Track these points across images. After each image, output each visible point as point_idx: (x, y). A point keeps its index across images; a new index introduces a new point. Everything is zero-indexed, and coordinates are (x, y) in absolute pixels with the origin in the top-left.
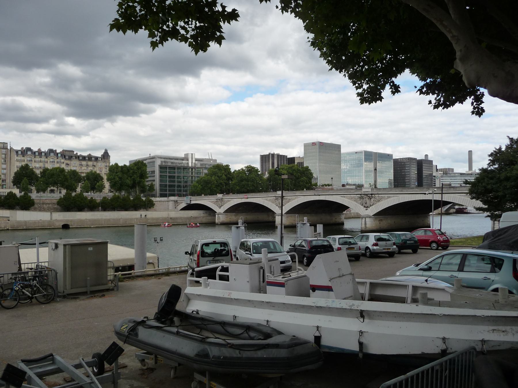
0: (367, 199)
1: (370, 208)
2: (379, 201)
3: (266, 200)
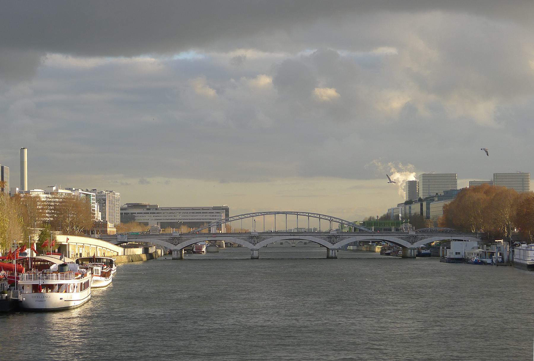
0: (334, 238)
2: (342, 240)
3: (238, 238)
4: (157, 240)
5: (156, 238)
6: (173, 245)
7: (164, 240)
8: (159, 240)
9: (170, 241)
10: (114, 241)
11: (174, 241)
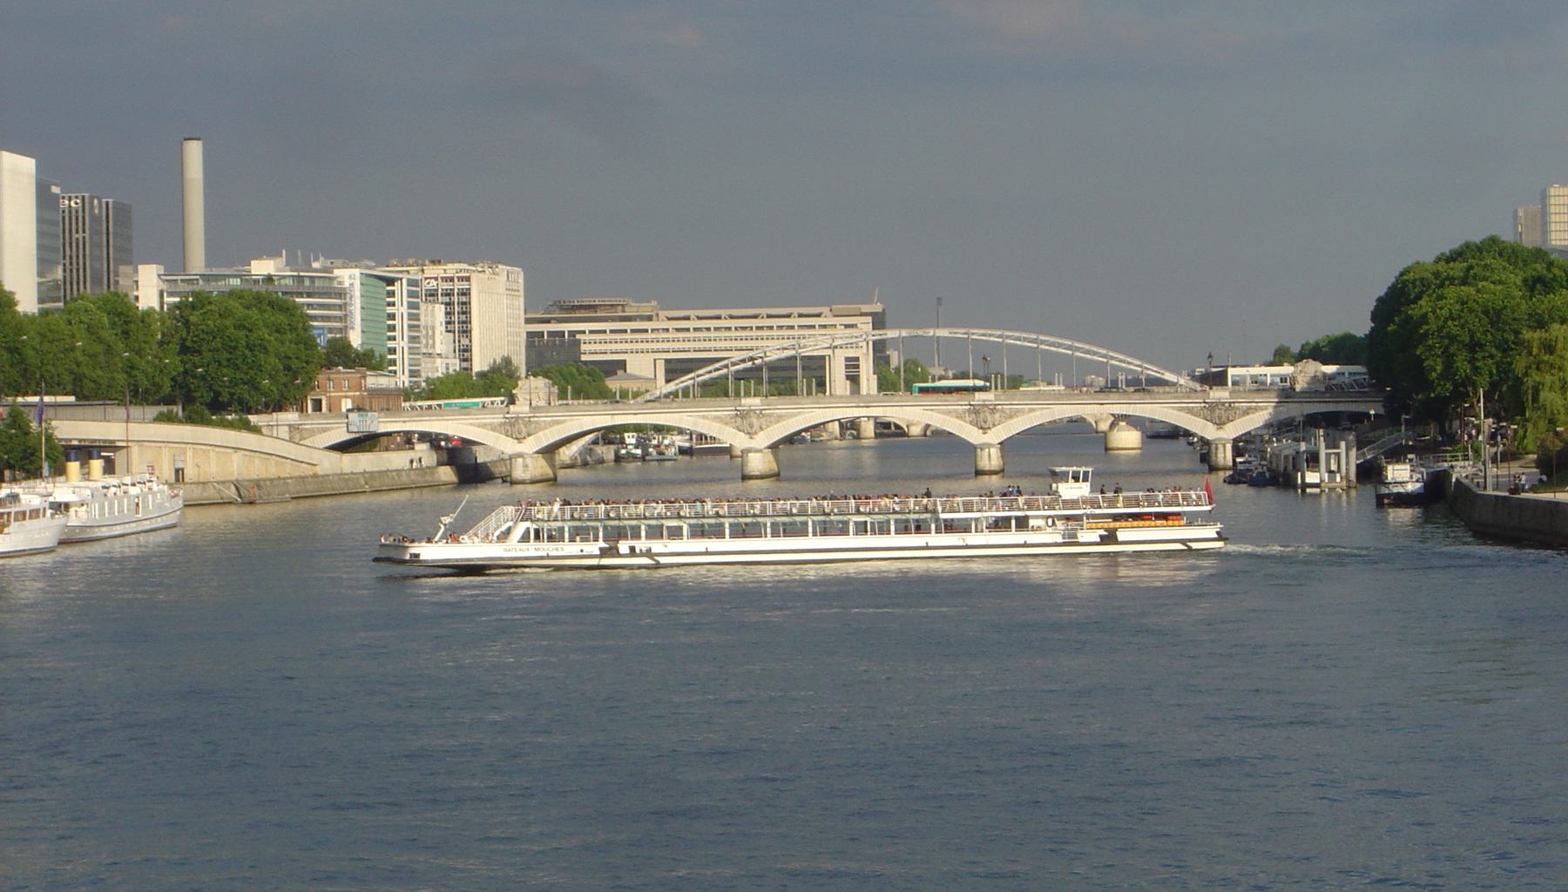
0: (988, 415)
1: (993, 429)
2: (1011, 417)
3: (704, 417)
5: (463, 421)
7: (485, 425)
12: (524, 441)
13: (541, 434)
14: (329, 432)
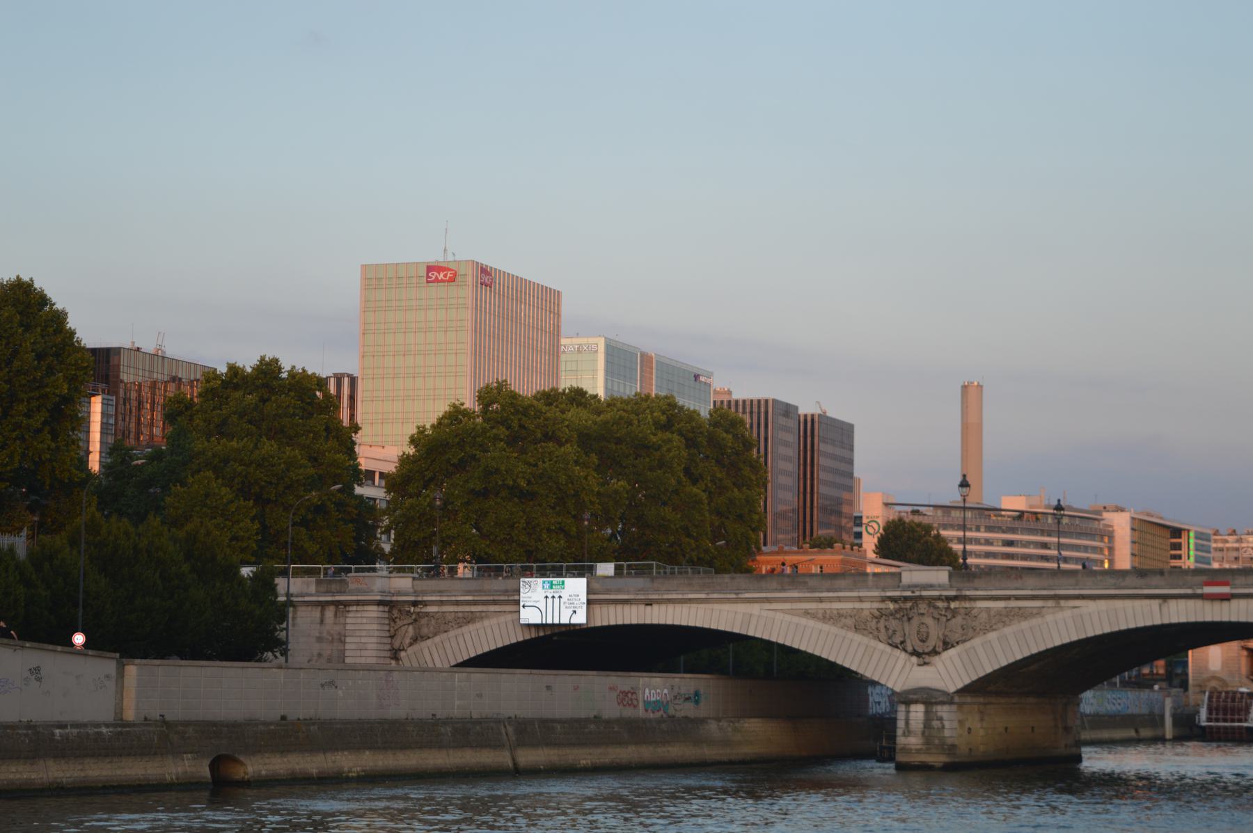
4: (788, 617)
5: (787, 606)
6: (903, 655)
8: (803, 621)
9: (882, 625)
10: (502, 619)
11: (911, 629)
12: (936, 659)
13: (977, 642)
14: (478, 625)
